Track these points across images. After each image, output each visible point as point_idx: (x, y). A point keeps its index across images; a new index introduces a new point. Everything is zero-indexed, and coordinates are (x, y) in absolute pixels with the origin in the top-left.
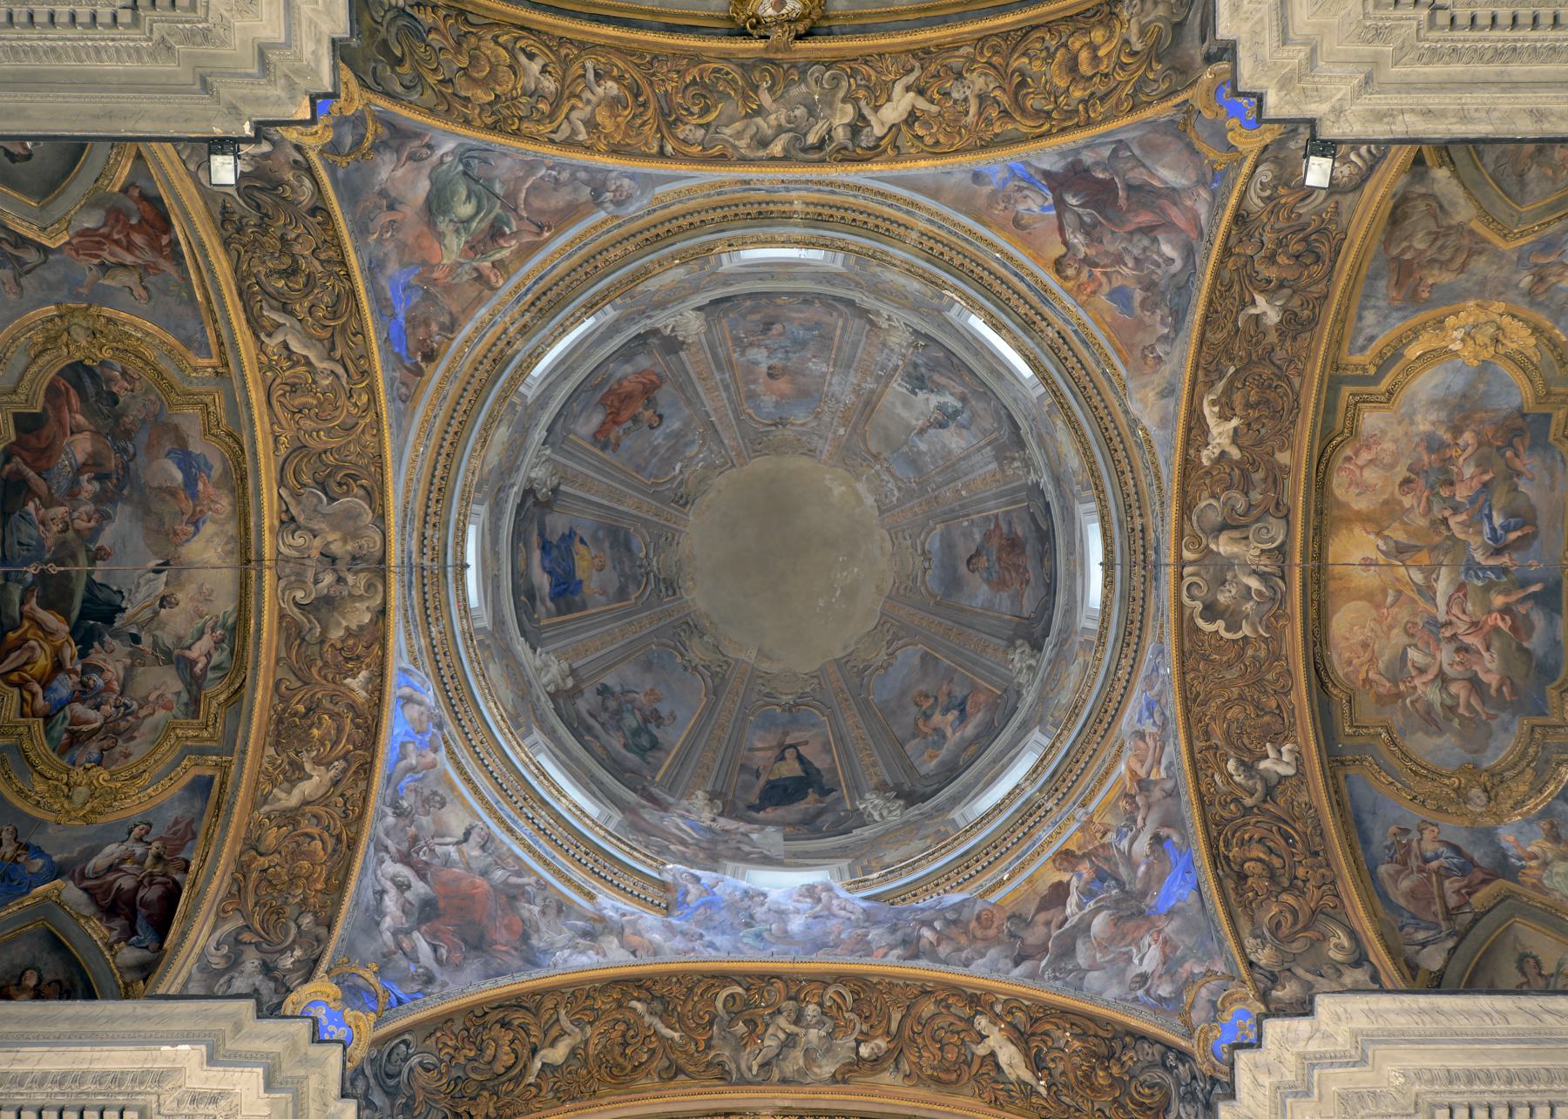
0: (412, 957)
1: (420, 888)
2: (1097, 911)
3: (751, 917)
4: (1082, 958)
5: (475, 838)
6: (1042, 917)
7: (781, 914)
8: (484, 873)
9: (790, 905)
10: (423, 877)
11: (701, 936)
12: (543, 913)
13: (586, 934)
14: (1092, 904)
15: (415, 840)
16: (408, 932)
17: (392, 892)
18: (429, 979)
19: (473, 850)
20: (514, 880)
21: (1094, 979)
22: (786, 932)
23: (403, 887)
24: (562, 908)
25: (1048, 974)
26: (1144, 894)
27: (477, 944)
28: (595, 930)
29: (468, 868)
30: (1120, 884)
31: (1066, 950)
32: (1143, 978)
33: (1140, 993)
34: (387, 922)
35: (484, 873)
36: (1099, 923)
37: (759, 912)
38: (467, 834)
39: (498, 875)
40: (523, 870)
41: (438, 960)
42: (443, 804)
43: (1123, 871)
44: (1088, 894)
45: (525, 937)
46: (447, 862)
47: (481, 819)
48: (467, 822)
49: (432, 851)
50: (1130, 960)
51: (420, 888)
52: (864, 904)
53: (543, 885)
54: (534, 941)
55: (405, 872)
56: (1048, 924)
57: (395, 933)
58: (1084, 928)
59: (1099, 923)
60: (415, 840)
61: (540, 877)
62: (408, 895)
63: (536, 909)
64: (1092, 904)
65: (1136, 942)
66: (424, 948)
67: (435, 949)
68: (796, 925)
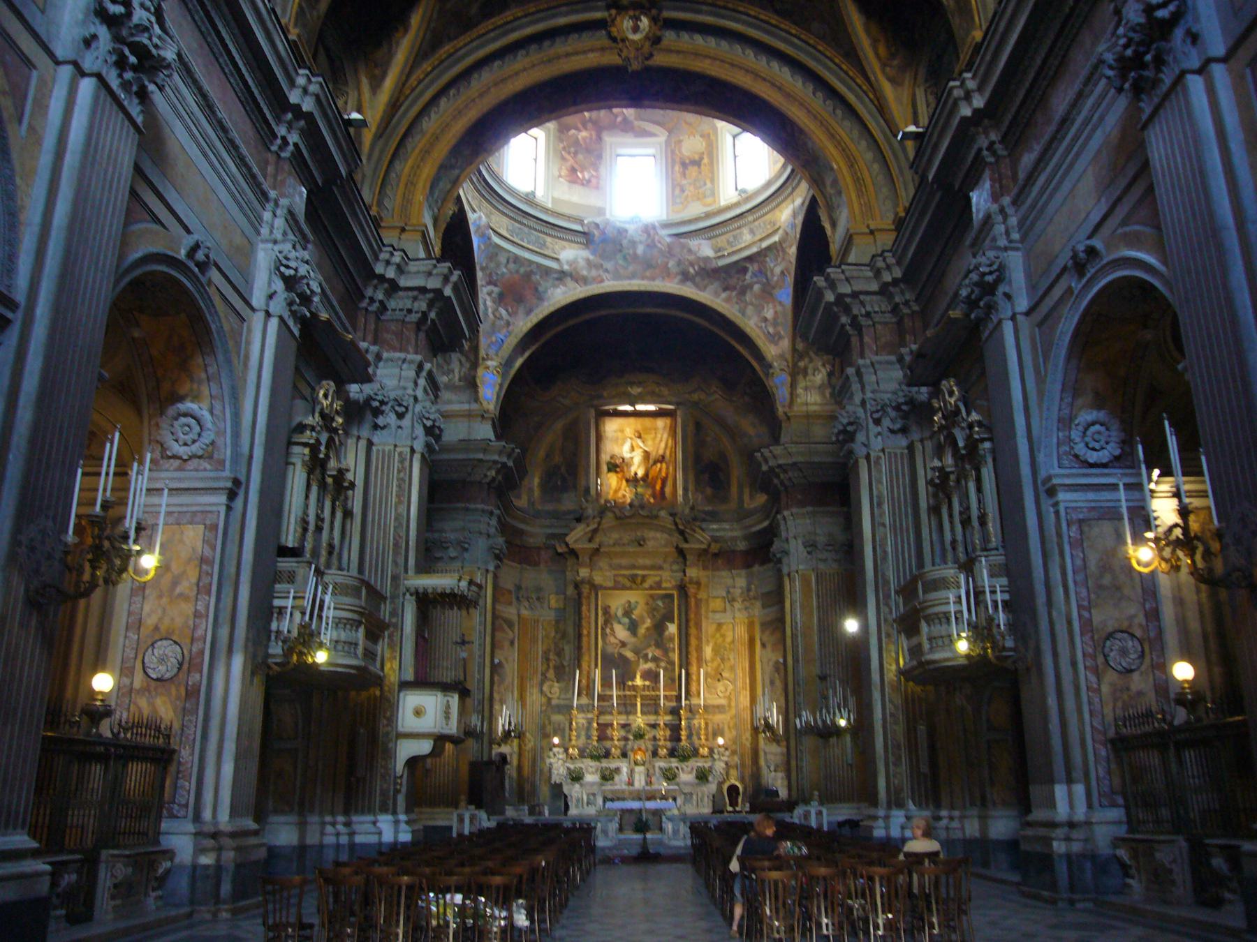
0: (501, 318)
1: (496, 290)
2: (756, 283)
3: (621, 245)
4: (748, 297)
5: (511, 260)
6: (737, 276)
7: (633, 243)
8: (517, 272)
9: (637, 239)
10: (495, 285)
11: (602, 265)
12: (541, 277)
13: (557, 279)
14: (755, 280)
15: (491, 274)
16: (496, 310)
17: (488, 298)
18: (508, 324)
19: (512, 266)
20: (529, 269)
21: (750, 310)
22: (635, 254)
23: (489, 294)
24: (547, 271)
25: (735, 300)
26: (774, 288)
27: (520, 299)
28: (562, 276)
29: (511, 272)
30: (767, 279)
31: (743, 291)
32: (765, 320)
33: (763, 325)
34: (490, 310)
35: (517, 272)
36: (757, 287)
37: (625, 242)
38: (508, 262)
39: (522, 270)
40: (531, 262)
41: (509, 314)
42: (497, 254)
43: (769, 274)
44: (754, 275)
45: (536, 289)
46: (503, 274)
47: (509, 252)
48: (506, 255)
49: (497, 274)
50: (763, 308)
51: (496, 290)
52: (668, 240)
53: (539, 265)
54: (540, 289)
55: (490, 288)
56: (738, 279)
57: (493, 314)
58: (750, 286)
59: (757, 287)
60: (491, 274)
61: (537, 263)
62: (494, 295)
63: (538, 277)
64: (755, 280)
65: (768, 303)
66: (503, 312)
67: (507, 311)
68: (640, 249)
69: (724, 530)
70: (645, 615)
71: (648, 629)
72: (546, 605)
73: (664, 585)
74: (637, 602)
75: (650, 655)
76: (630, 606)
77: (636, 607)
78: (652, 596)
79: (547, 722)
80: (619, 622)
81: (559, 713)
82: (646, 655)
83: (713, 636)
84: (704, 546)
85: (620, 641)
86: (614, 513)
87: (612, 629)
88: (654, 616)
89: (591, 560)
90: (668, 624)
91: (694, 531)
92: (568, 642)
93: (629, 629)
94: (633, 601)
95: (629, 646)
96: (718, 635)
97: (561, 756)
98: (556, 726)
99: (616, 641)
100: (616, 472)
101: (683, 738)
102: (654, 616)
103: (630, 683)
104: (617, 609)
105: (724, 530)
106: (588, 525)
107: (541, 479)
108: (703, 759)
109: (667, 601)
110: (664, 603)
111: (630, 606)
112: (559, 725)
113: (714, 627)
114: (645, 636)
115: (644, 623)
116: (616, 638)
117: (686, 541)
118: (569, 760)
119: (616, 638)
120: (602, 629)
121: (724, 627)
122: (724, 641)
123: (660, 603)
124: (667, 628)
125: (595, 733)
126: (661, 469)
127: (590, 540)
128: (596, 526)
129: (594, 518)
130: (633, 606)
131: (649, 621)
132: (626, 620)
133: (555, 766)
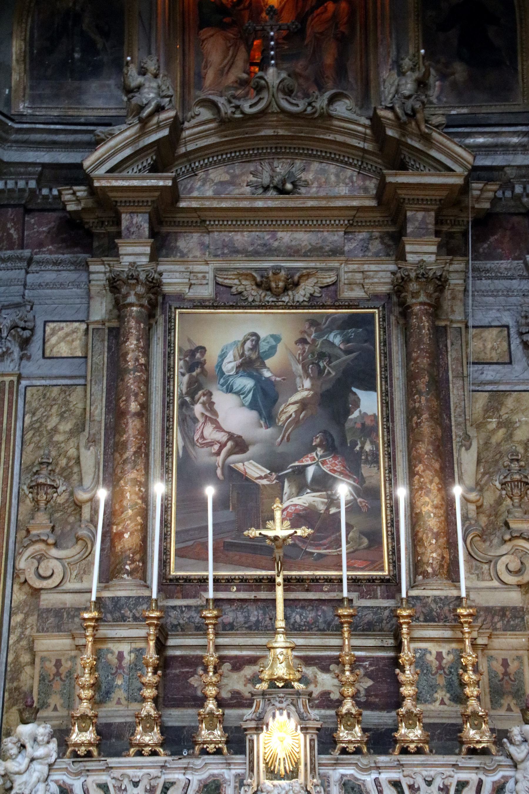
69: (506, 148)
70: (298, 368)
71: (303, 404)
72: (35, 348)
73: (347, 294)
74: (277, 339)
75: (310, 472)
76: (255, 347)
77: (272, 350)
78: (313, 322)
79: (25, 658)
80: (230, 390)
81: (58, 628)
82: (301, 471)
83: (479, 426)
84: (459, 181)
85: (231, 436)
86: (213, 105)
87: (210, 405)
88: (321, 372)
89: (153, 234)
90: (360, 393)
91: (426, 138)
92: (92, 441)
93: (253, 406)
94: (263, 334)
95: (252, 450)
96: (493, 423)
97: (40, 752)
98: (50, 666)
99: (222, 437)
100: (223, 27)
101: (407, 690)
102: (321, 372)
103: (254, 533)
104: (223, 356)
105: (506, 148)
106: (143, 133)
107: (30, 43)
108: (475, 761)
109: (351, 332)
110: (346, 340)
111: (255, 347)
112: (58, 664)
113: (482, 399)
114: (297, 422)
115: (295, 391)
116: (219, 428)
117: (403, 167)
118: (67, 761)
119: (219, 428)
120: (183, 404)
121: (510, 402)
122: (509, 437)
123: (336, 339)
124: (357, 404)
125: (150, 677)
126: (335, 16)
127: (154, 169)
128: (165, 132)
129: (159, 109)
130: (264, 347)
131: (307, 383)
132: (248, 383)
133: (18, 781)
